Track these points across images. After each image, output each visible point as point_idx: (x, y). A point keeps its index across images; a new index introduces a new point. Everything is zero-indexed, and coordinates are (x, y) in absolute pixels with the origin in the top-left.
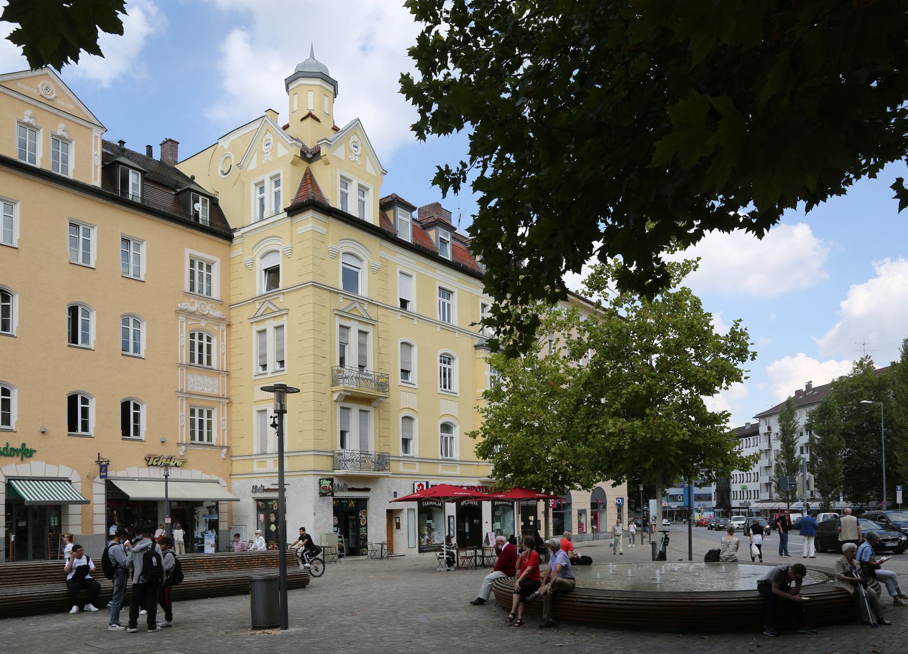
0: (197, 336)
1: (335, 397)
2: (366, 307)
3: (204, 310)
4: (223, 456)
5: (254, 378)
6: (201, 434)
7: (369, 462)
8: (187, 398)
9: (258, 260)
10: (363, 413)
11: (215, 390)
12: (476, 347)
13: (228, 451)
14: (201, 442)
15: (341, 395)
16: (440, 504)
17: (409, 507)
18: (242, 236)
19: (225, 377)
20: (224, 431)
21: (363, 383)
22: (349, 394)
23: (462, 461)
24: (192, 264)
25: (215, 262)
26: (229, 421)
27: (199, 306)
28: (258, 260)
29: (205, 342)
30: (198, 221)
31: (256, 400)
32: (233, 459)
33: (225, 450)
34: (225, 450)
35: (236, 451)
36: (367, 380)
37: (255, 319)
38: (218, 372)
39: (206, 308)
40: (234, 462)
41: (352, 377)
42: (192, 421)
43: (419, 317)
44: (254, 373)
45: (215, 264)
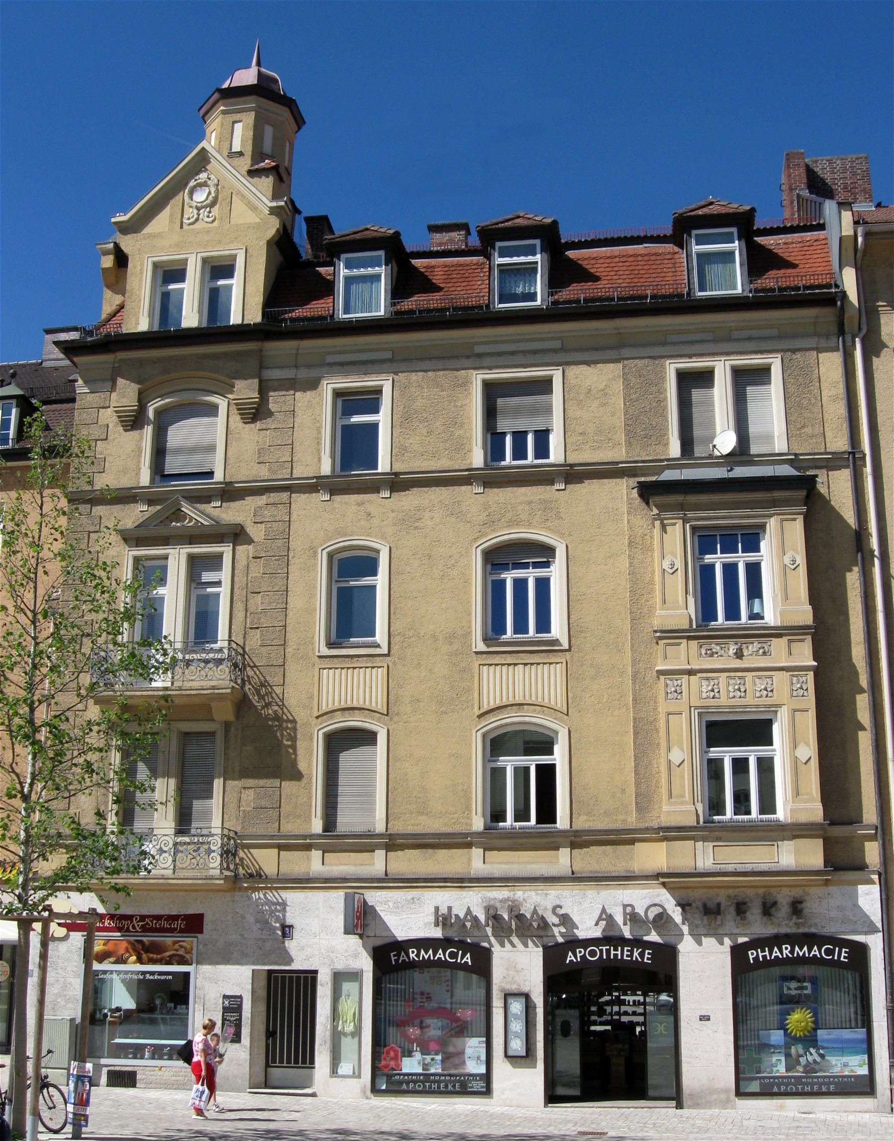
16: (468, 959)
17: (340, 966)
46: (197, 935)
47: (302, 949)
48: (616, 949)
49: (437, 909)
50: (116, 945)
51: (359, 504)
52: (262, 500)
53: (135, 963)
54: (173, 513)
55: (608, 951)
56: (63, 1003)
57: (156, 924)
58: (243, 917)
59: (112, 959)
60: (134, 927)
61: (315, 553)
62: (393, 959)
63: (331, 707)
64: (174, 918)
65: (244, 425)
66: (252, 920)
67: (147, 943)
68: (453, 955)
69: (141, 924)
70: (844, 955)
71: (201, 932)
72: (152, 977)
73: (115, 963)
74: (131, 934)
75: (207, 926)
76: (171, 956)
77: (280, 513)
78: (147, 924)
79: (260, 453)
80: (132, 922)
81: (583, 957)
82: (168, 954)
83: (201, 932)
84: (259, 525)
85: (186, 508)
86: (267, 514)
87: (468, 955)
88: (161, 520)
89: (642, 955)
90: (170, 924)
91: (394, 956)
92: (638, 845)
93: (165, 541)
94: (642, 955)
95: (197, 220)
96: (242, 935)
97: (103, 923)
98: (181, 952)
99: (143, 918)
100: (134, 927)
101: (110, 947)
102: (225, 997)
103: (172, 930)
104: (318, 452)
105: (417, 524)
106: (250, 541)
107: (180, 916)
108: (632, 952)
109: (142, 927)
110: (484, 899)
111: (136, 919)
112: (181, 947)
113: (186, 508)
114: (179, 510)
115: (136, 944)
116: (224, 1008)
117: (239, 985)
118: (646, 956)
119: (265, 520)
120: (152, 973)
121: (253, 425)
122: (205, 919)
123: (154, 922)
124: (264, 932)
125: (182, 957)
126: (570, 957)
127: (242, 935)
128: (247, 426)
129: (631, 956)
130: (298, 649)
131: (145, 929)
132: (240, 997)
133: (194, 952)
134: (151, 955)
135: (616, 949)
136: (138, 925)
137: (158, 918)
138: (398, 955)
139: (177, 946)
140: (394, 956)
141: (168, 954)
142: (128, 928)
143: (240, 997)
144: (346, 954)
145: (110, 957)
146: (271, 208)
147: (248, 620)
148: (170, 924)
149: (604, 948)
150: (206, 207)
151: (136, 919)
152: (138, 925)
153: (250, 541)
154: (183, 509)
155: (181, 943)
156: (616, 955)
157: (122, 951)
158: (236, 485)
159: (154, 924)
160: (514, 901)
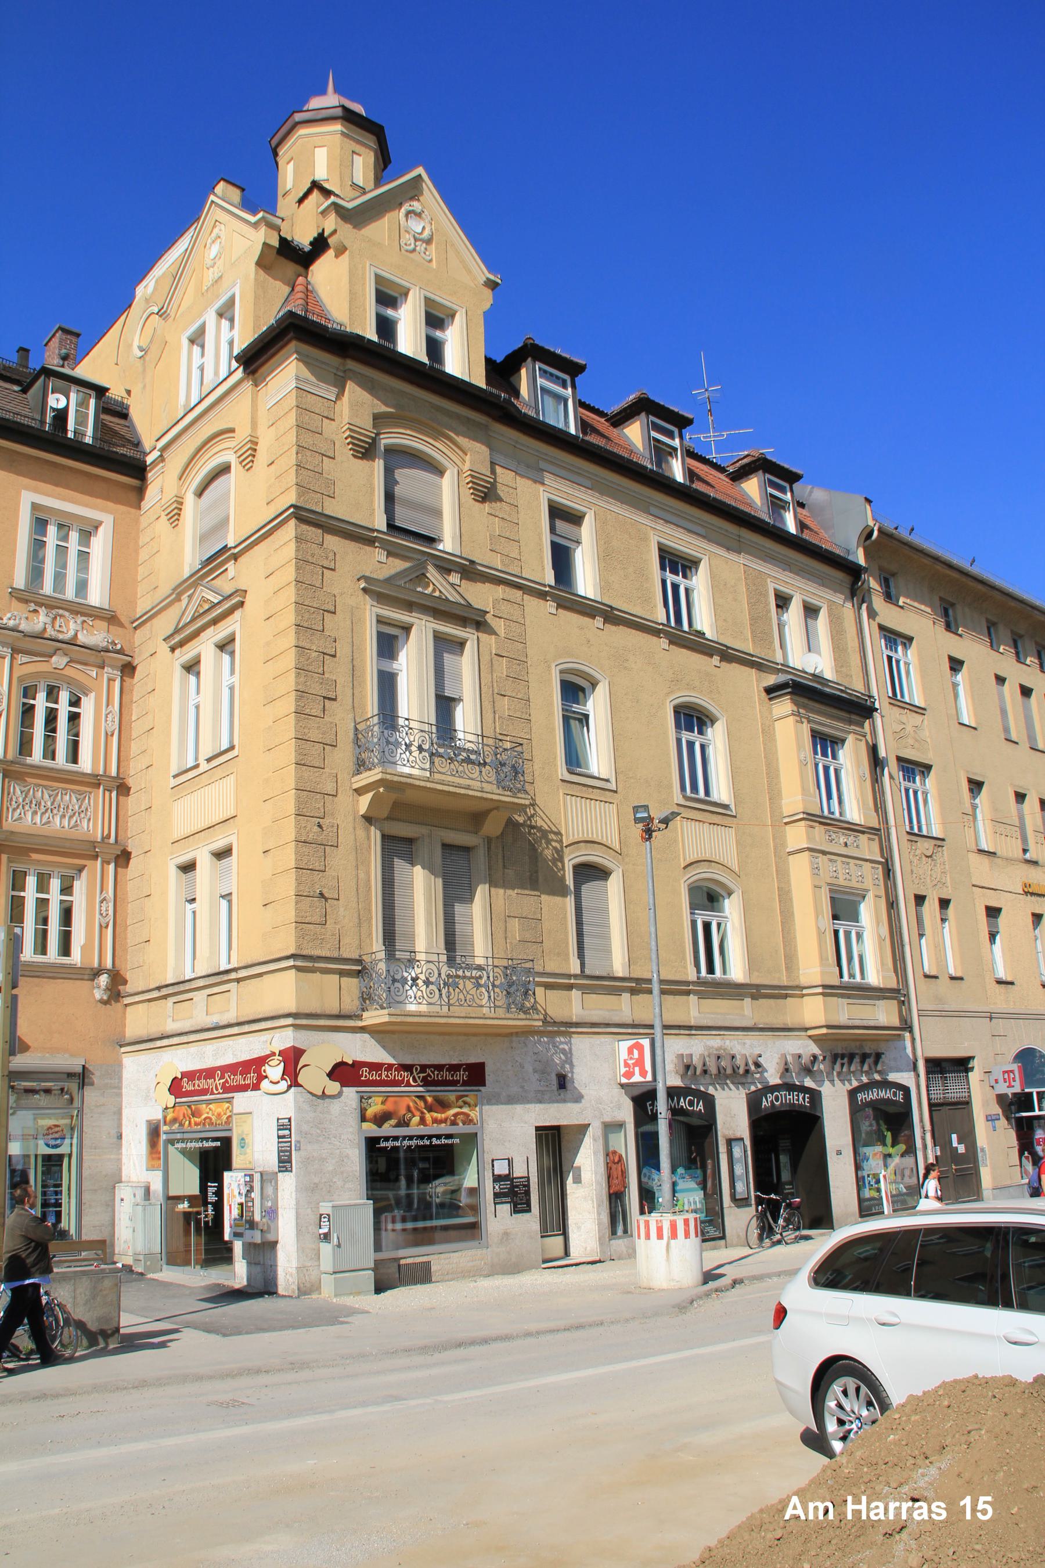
2: (455, 578)
3: (64, 629)
4: (98, 994)
5: (173, 782)
9: (190, 499)
12: (769, 691)
16: (701, 1106)
17: (608, 1119)
18: (161, 458)
24: (40, 524)
25: (101, 523)
27: (48, 620)
28: (190, 499)
30: (66, 433)
31: (176, 837)
35: (135, 982)
37: (179, 640)
38: (94, 781)
39: (67, 626)
43: (611, 616)
44: (174, 770)
45: (101, 530)
46: (481, 1088)
48: (789, 1095)
50: (395, 1102)
51: (581, 628)
52: (500, 591)
54: (417, 577)
55: (785, 1095)
56: (340, 1183)
57: (438, 1075)
58: (522, 1066)
59: (393, 1122)
60: (415, 1080)
61: (549, 667)
62: (649, 1108)
63: (576, 839)
64: (454, 1068)
65: (474, 502)
66: (531, 1070)
68: (691, 1103)
69: (421, 1075)
71: (483, 1084)
72: (438, 1142)
73: (396, 1126)
74: (412, 1089)
75: (489, 1078)
76: (455, 1115)
77: (516, 613)
78: (429, 1075)
79: (491, 540)
80: (412, 1073)
81: (772, 1101)
83: (483, 1084)
84: (498, 619)
85: (432, 573)
86: (505, 609)
87: (701, 1103)
88: (410, 578)
89: (804, 1098)
90: (452, 1076)
91: (650, 1105)
92: (805, 998)
93: (410, 606)
94: (804, 1098)
95: (414, 250)
96: (522, 1087)
97: (380, 1075)
99: (423, 1068)
103: (454, 1083)
104: (542, 558)
105: (626, 665)
106: (492, 632)
107: (462, 1065)
108: (798, 1096)
109: (424, 1079)
111: (416, 1069)
112: (465, 1103)
113: (432, 573)
114: (424, 575)
115: (417, 1100)
118: (807, 1100)
119: (503, 616)
121: (481, 506)
122: (486, 1068)
123: (436, 1072)
124: (542, 1083)
125: (468, 1115)
126: (764, 1103)
127: (522, 1087)
128: (477, 504)
129: (798, 1100)
130: (543, 769)
134: (435, 1115)
135: (789, 1095)
137: (439, 1067)
139: (460, 1102)
140: (650, 1105)
142: (408, 1081)
144: (611, 1105)
145: (390, 1119)
146: (488, 279)
147: (497, 724)
148: (452, 1076)
149: (783, 1093)
150: (423, 241)
151: (416, 1069)
152: (419, 1077)
153: (492, 632)
154: (428, 575)
155: (465, 1099)
156: (790, 1099)
157: (402, 1111)
158: (480, 568)
159: (436, 1075)
160: (725, 1050)
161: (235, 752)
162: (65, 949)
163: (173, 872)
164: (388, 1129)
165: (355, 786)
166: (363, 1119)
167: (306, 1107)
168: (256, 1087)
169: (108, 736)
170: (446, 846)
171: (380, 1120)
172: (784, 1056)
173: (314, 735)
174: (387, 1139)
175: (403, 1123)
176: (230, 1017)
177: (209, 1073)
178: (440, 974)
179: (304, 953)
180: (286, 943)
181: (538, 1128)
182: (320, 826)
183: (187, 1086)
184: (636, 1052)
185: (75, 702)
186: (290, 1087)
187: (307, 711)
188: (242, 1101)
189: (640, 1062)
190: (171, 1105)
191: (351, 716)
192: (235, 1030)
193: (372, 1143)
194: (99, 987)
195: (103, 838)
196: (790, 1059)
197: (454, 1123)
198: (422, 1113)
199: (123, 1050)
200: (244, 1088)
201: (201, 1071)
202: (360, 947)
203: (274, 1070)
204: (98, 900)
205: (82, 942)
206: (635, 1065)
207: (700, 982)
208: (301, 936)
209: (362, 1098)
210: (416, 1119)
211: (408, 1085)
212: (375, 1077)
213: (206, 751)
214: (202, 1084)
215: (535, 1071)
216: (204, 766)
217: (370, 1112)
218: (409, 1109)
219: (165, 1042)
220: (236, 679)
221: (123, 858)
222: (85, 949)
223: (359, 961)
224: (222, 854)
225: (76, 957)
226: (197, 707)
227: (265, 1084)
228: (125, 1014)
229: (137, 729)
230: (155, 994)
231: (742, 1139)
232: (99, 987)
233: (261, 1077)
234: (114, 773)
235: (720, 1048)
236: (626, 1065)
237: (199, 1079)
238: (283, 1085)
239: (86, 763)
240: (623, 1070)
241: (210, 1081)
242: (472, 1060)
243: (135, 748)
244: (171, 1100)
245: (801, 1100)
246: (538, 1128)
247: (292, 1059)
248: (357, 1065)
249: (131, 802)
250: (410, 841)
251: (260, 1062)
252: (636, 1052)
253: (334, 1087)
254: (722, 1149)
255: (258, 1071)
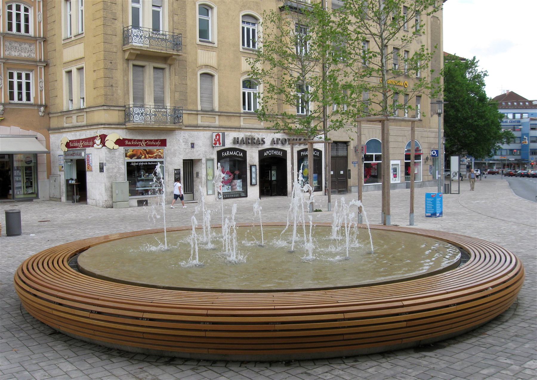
0: (14, 7)
1: (127, 55)
5: (63, 42)
6: (20, 94)
7: (160, 115)
8: (4, 63)
10: (138, 69)
11: (33, 55)
13: (45, 109)
14: (28, 102)
15: (130, 53)
17: (208, 157)
19: (42, 43)
20: (41, 91)
21: (154, 43)
22: (139, 52)
23: (221, 112)
26: (46, 82)
29: (22, 13)
32: (51, 116)
33: (42, 109)
34: (42, 109)
35: (52, 109)
36: (158, 39)
40: (51, 119)
41: (142, 36)
42: (11, 84)
44: (63, 37)
47: (197, 152)
49: (264, 138)
50: (136, 151)
53: (144, 158)
56: (119, 176)
59: (136, 157)
60: (143, 144)
64: (156, 141)
66: (182, 141)
67: (148, 151)
68: (238, 153)
70: (318, 154)
73: (137, 158)
75: (168, 144)
82: (155, 155)
94: (280, 153)
96: (179, 147)
98: (160, 154)
99: (146, 141)
100: (143, 144)
101: (134, 153)
102: (175, 170)
103: (156, 145)
110: (245, 135)
112: (159, 152)
116: (175, 174)
117: (179, 165)
120: (150, 162)
125: (160, 155)
126: (265, 154)
127: (179, 147)
131: (147, 145)
132: (180, 169)
133: (164, 153)
136: (144, 143)
137: (151, 141)
138: (224, 153)
139: (158, 152)
141: (155, 155)
143: (180, 169)
155: (160, 150)
157: (139, 154)
161: (84, 35)
162: (28, 99)
163: (64, 74)
164: (134, 160)
165: (124, 49)
166: (126, 156)
167: (108, 153)
168: (93, 146)
169: (40, 23)
170: (155, 68)
171: (131, 157)
172: (273, 139)
173: (109, 32)
174: (134, 162)
175: (139, 158)
176: (84, 123)
177: (78, 141)
178: (150, 112)
179: (107, 105)
180: (101, 101)
181: (184, 160)
182: (111, 63)
183: (71, 145)
184: (218, 137)
185: (26, 10)
186: (102, 146)
187: (107, 24)
188: (88, 150)
189: (219, 140)
190: (66, 150)
191: (122, 25)
192: (86, 128)
193: (129, 164)
194: (41, 111)
195: (39, 60)
196: (275, 140)
197: (156, 158)
198: (145, 155)
199: (50, 132)
200: (89, 146)
201: (75, 140)
202: (125, 103)
203: (98, 141)
204: (39, 82)
205: (34, 96)
206: (217, 141)
207: (245, 113)
208: (106, 99)
209: (126, 150)
210: (143, 157)
211: (141, 146)
212: (130, 143)
213: (74, 33)
214: (76, 144)
215: (183, 142)
216: (73, 38)
217: (128, 154)
218: (141, 153)
219: (64, 130)
220: (83, 8)
221: (47, 66)
222: (36, 98)
223: (125, 106)
224: (80, 69)
225: (32, 101)
226: (70, 15)
227: (95, 145)
228: (50, 120)
229: (50, 20)
230: (60, 114)
231: (256, 166)
232: (41, 111)
233: (94, 143)
234: (42, 36)
235: (250, 136)
236: (215, 141)
237: (75, 143)
238: (101, 146)
239: (31, 32)
240: (214, 142)
241: (78, 144)
242: (162, 138)
243: (49, 27)
244: (66, 149)
245: (280, 154)
246: (184, 160)
247: (103, 138)
248: (124, 140)
249: (51, 69)
250: (143, 67)
251: (94, 138)
252: (218, 137)
253: (116, 147)
254: (248, 168)
255: (93, 141)
